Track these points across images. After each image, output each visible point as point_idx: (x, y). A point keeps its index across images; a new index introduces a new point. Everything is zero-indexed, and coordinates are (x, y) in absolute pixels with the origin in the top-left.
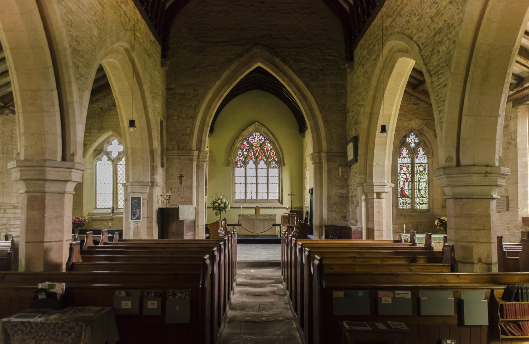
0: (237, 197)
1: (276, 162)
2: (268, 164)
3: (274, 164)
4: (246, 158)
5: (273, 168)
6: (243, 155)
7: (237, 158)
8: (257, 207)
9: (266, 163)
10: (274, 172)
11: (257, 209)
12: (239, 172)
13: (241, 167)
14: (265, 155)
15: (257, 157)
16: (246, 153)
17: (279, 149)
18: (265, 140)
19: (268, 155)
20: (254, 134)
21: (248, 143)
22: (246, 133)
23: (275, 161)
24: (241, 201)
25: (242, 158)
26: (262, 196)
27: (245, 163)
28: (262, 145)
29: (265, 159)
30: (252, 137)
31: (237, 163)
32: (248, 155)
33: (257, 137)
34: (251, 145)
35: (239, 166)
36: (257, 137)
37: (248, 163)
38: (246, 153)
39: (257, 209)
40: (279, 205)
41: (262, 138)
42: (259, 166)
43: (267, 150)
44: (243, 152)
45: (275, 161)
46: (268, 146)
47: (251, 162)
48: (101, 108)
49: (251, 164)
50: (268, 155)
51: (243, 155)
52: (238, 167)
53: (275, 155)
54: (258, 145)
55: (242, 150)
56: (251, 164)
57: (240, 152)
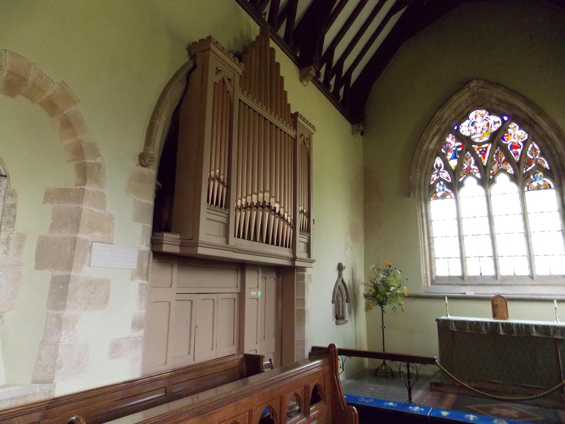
1: (548, 173)
2: (521, 178)
3: (541, 180)
4: (454, 173)
5: (539, 188)
6: (447, 167)
7: (434, 177)
8: (498, 297)
9: (514, 178)
11: (498, 304)
12: (440, 210)
13: (443, 197)
14: (509, 159)
15: (485, 167)
16: (453, 163)
17: (552, 134)
18: (504, 122)
19: (517, 158)
20: (472, 115)
21: (459, 137)
22: (447, 113)
24: (450, 281)
25: (445, 175)
27: (454, 186)
29: (510, 170)
30: (467, 123)
31: (432, 189)
32: (460, 165)
34: (467, 142)
35: (439, 195)
36: (479, 119)
37: (461, 185)
38: (453, 163)
39: (499, 302)
41: (494, 118)
43: (514, 146)
46: (516, 134)
49: (471, 184)
50: (517, 158)
51: (447, 167)
52: (436, 198)
53: (542, 154)
54: (486, 138)
55: (444, 157)
56: (471, 184)
57: (439, 161)
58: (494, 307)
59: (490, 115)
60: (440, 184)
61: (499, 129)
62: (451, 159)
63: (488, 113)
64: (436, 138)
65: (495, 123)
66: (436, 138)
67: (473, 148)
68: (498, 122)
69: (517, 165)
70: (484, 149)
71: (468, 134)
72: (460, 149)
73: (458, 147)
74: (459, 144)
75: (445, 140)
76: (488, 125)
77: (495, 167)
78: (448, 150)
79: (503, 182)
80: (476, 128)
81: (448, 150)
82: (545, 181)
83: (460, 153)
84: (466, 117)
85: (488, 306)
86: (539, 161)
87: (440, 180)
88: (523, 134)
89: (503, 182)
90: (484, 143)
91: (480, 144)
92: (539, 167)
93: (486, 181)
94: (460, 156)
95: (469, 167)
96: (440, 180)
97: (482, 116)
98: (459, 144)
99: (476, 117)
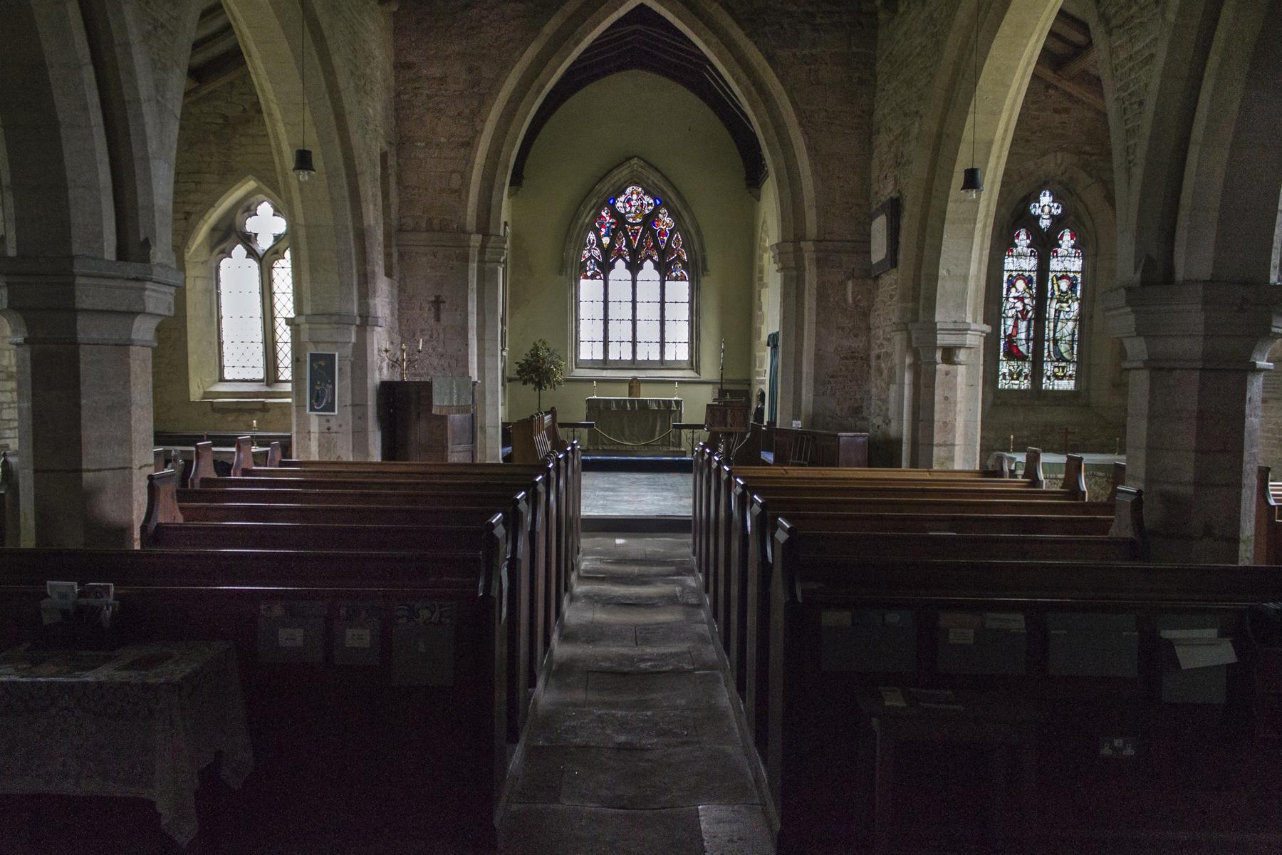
0: (585, 354)
1: (685, 266)
2: (664, 270)
4: (607, 252)
5: (676, 279)
6: (600, 244)
8: (635, 379)
9: (657, 266)
10: (679, 290)
11: (634, 384)
12: (589, 289)
13: (593, 277)
14: (656, 247)
16: (606, 241)
17: (692, 231)
18: (656, 206)
19: (663, 246)
20: (629, 191)
21: (614, 213)
22: (606, 187)
24: (593, 364)
25: (597, 252)
26: (649, 352)
27: (605, 267)
28: (649, 220)
29: (656, 258)
30: (622, 198)
31: (583, 265)
32: (612, 244)
33: (635, 197)
34: (620, 219)
35: (589, 274)
36: (635, 197)
37: (612, 266)
38: (606, 241)
40: (689, 374)
41: (648, 200)
42: (640, 275)
43: (662, 233)
44: (599, 238)
46: (666, 221)
47: (620, 264)
48: (225, 118)
49: (620, 270)
50: (663, 246)
51: (600, 244)
52: (586, 277)
54: (638, 220)
55: (597, 232)
56: (620, 270)
57: (592, 236)
58: (631, 388)
61: (653, 211)
69: (662, 254)
77: (643, 252)
78: (602, 225)
79: (649, 270)
81: (602, 225)
85: (626, 387)
87: (591, 257)
89: (649, 270)
90: (636, 224)
91: (633, 225)
94: (613, 234)
96: (591, 257)
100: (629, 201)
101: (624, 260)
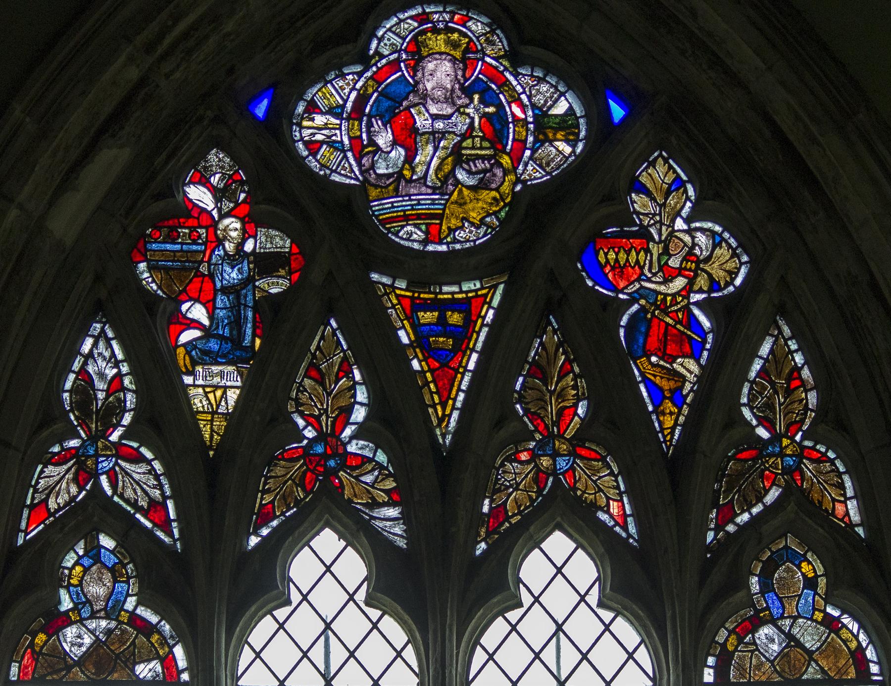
7: (56, 485)
9: (634, 583)
14: (617, 427)
16: (215, 391)
18: (603, 131)
19: (670, 423)
20: (390, 36)
21: (278, 186)
23: (832, 539)
25: (141, 480)
28: (552, 239)
29: (616, 510)
32: (262, 416)
33: (439, 74)
34: (332, 228)
36: (439, 74)
37: (261, 586)
38: (215, 391)
44: (158, 374)
45: (832, 539)
46: (682, 245)
47: (327, 569)
50: (670, 423)
51: (163, 416)
53: (832, 422)
55: (148, 330)
57: (102, 358)
59: (515, 59)
60: (94, 551)
61: (572, 177)
62: (202, 356)
63: (501, 44)
64: (112, 159)
65: (545, 126)
66: (112, 159)
67: (372, 297)
68: (567, 124)
69: (670, 481)
70: (455, 318)
71: (346, 173)
72: (276, 286)
73: (266, 264)
74: (277, 241)
75: (171, 189)
76: (496, 127)
77: (516, 472)
78: (189, 278)
80: (408, 138)
82: (832, 624)
83: (270, 307)
84: (347, 44)
86: (808, 467)
87: (92, 514)
88: (722, 252)
90: (456, 265)
91: (424, 270)
92: (803, 511)
93: (443, 588)
94: (271, 345)
95: (330, 438)
96: (92, 514)
97: (465, 58)
98: (277, 241)
99: (417, 53)
100: (394, 106)
101: (359, 532)
